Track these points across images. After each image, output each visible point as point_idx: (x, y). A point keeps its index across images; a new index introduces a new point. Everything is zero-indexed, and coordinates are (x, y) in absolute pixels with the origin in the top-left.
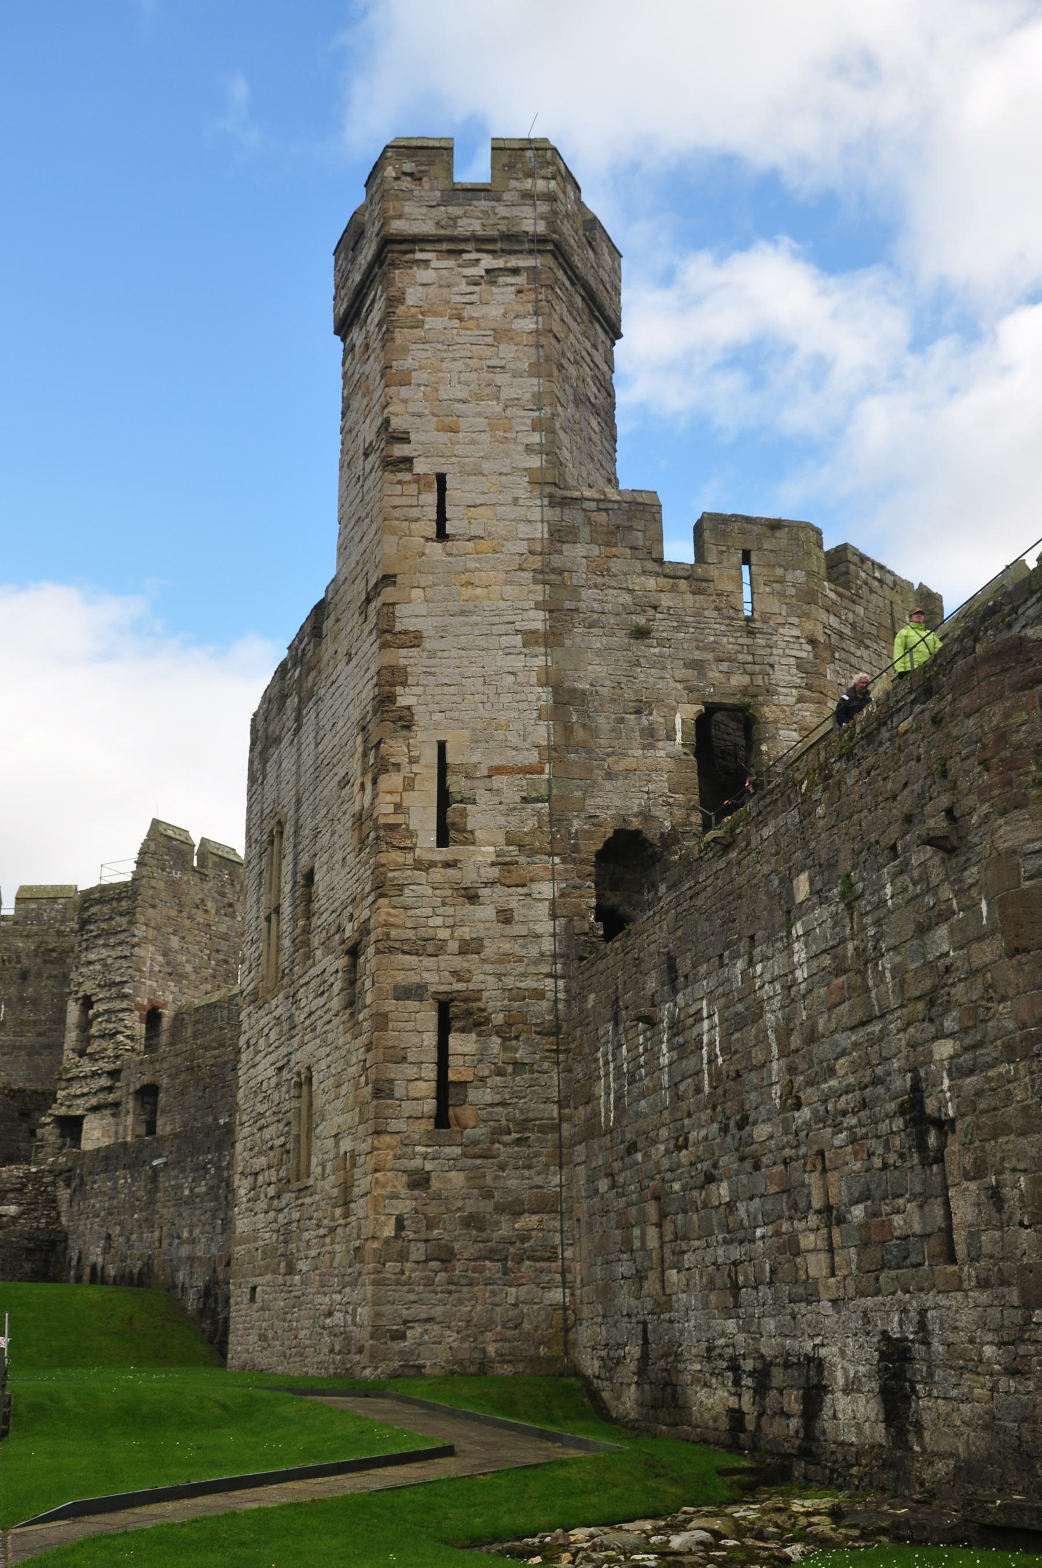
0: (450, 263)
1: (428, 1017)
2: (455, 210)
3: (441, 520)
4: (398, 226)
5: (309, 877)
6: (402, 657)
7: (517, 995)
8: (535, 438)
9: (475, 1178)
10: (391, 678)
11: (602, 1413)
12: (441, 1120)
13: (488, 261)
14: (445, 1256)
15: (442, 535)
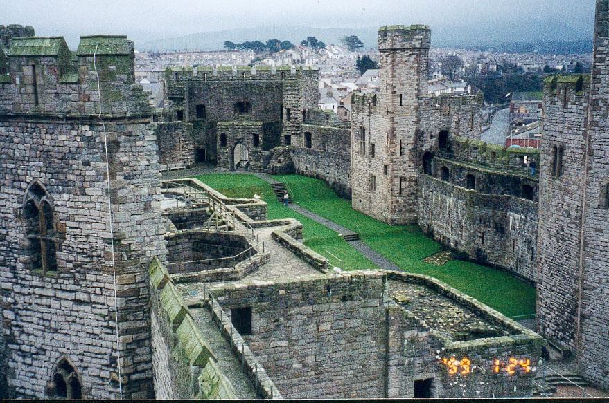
0: (402, 53)
1: (398, 179)
2: (404, 43)
3: (401, 102)
4: (394, 47)
5: (373, 145)
6: (395, 126)
7: (410, 177)
8: (417, 87)
9: (405, 201)
10: (393, 129)
11: (422, 231)
12: (400, 193)
13: (410, 53)
14: (401, 211)
15: (401, 105)
